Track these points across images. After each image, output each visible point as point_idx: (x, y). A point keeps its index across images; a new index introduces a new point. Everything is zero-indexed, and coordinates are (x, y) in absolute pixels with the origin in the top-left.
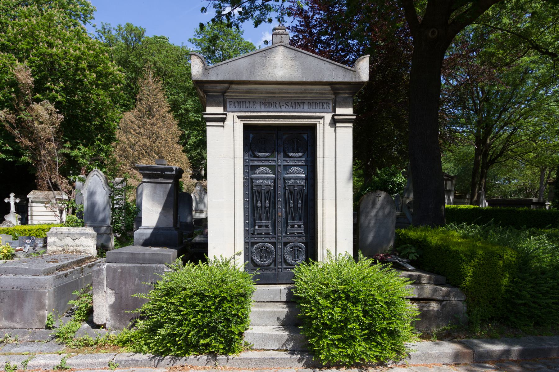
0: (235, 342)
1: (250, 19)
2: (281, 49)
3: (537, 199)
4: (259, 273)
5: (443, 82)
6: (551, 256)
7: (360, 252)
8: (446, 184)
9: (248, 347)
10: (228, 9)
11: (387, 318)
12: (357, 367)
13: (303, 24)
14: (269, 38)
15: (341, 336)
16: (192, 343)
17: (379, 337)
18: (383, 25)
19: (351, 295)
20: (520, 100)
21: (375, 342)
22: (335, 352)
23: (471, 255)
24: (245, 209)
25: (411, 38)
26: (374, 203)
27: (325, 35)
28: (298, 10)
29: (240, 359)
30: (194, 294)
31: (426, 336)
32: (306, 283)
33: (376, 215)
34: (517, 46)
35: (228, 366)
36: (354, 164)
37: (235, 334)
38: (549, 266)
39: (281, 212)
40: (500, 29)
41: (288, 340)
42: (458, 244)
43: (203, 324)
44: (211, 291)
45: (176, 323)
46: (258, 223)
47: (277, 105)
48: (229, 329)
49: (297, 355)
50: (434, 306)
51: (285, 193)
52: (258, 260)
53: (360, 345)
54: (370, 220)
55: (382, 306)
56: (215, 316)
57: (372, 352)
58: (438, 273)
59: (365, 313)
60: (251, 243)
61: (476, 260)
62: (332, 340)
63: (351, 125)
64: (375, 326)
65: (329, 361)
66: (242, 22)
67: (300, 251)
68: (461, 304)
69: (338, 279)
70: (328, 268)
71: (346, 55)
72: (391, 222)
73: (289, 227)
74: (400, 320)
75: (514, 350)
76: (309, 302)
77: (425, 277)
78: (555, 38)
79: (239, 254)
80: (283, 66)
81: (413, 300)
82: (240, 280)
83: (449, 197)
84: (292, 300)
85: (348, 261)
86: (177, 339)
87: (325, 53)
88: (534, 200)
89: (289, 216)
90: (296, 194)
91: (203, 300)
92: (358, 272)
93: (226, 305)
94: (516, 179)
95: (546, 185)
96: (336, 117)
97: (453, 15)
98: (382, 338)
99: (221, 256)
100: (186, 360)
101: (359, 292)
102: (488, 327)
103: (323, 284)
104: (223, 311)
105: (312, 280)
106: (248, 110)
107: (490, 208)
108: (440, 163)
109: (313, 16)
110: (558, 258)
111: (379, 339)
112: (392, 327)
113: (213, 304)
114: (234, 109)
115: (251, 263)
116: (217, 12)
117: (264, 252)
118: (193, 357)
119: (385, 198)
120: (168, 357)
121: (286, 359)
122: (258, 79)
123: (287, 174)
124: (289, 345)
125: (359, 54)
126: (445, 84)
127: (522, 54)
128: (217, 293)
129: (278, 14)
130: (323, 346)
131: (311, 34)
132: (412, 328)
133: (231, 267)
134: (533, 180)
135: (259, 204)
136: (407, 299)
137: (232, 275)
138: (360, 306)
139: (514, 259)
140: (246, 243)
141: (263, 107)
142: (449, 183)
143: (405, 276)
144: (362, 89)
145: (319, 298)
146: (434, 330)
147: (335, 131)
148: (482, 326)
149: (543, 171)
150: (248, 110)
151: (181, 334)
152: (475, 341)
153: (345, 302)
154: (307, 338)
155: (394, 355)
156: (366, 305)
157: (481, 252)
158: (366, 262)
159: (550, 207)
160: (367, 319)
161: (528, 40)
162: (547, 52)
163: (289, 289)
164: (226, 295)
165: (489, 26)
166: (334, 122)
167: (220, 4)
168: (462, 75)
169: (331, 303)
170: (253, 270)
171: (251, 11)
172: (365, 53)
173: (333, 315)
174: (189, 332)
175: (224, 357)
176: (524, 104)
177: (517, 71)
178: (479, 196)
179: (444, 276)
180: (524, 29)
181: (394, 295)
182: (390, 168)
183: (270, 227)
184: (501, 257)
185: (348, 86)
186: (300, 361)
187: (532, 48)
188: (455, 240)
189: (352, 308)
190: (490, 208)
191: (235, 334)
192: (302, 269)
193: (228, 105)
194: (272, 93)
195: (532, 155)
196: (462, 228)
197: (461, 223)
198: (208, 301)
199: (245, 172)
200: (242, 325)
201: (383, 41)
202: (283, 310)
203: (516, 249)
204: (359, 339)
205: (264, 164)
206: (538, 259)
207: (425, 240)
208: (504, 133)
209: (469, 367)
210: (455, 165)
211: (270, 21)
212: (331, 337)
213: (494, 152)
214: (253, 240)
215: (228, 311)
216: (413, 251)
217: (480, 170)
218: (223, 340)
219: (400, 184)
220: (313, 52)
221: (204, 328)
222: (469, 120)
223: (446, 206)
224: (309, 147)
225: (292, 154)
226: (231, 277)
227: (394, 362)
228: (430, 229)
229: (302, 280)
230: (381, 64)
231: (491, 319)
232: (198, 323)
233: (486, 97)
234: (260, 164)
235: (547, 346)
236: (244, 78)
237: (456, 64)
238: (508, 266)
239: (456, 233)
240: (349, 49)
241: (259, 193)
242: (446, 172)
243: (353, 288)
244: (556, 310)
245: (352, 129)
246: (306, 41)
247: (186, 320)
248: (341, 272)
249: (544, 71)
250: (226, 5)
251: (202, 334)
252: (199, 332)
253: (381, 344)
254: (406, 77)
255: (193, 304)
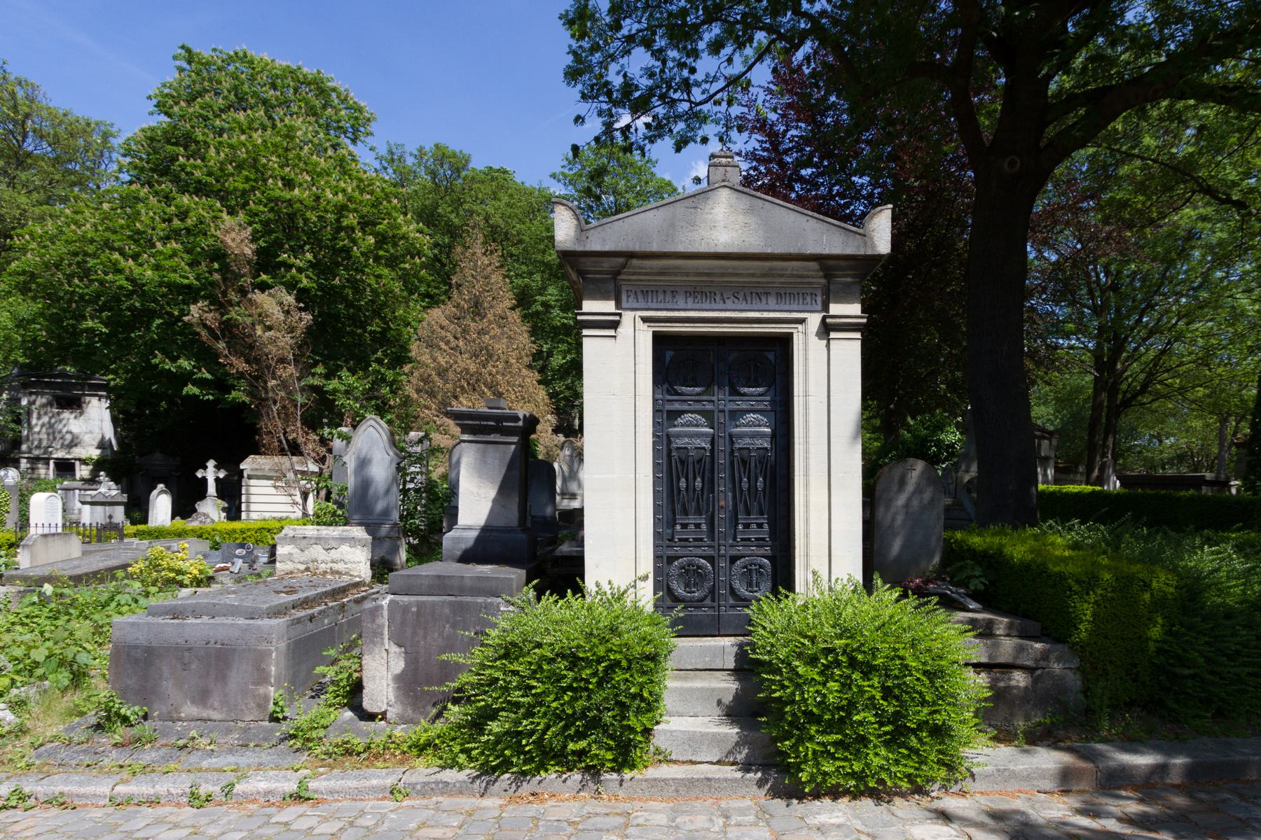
0: (635, 747)
1: (667, 138)
2: (724, 194)
3: (1213, 475)
4: (681, 615)
5: (1031, 256)
6: (1244, 584)
7: (876, 576)
8: (1039, 445)
9: (661, 757)
10: (625, 119)
11: (928, 702)
12: (871, 796)
13: (767, 145)
14: (702, 172)
15: (839, 737)
16: (552, 749)
17: (913, 738)
18: (917, 148)
19: (860, 657)
20: (1178, 288)
21: (907, 748)
22: (828, 767)
23: (1090, 582)
24: (656, 493)
25: (970, 173)
26: (902, 483)
27: (805, 167)
28: (758, 121)
29: (646, 780)
30: (557, 655)
31: (1003, 736)
32: (772, 634)
33: (907, 505)
34: (1171, 189)
35: (621, 794)
36: (865, 406)
37: (636, 733)
38: (1240, 603)
39: (724, 498)
40: (1138, 157)
41: (737, 744)
42: (1064, 560)
43: (574, 713)
44: (590, 650)
45: (522, 710)
46: (680, 519)
47: (718, 298)
48: (625, 723)
49: (756, 772)
50: (1019, 679)
51: (732, 463)
52: (680, 591)
53: (876, 754)
54: (896, 513)
55: (918, 679)
56: (598, 698)
57: (901, 768)
58: (1025, 616)
59: (887, 693)
60: (668, 557)
61: (1099, 592)
62: (823, 744)
63: (858, 335)
64: (905, 717)
65: (818, 785)
66: (652, 142)
67: (761, 574)
68: (1070, 674)
69: (833, 627)
70: (815, 607)
71: (847, 205)
72: (935, 519)
73: (740, 527)
74: (954, 705)
75: (1175, 765)
76: (778, 671)
77: (1002, 623)
78: (1243, 173)
79: (645, 578)
80: (728, 224)
81: (978, 667)
82: (647, 629)
83: (1045, 471)
84: (746, 668)
85: (854, 591)
86: (524, 742)
87: (809, 200)
88: (1209, 476)
89: (741, 507)
90: (753, 465)
91: (575, 666)
92: (872, 613)
93: (619, 676)
94: (1174, 437)
95: (1230, 447)
96: (828, 320)
97: (1051, 131)
98: (920, 740)
99: (610, 583)
100: (540, 782)
101: (874, 651)
102: (1124, 719)
103: (805, 637)
104: (614, 687)
105: (786, 629)
106: (662, 306)
107: (1123, 491)
108: (1028, 407)
109: (786, 131)
110: (1256, 588)
111: (914, 742)
112: (939, 719)
113: (595, 674)
114: (635, 306)
115: (667, 596)
116: (604, 124)
117: (692, 575)
118: (554, 776)
119: (923, 473)
120: (507, 776)
121: (735, 780)
122: (681, 248)
123: (737, 426)
124: (740, 753)
125: (874, 203)
126: (1036, 258)
127: (1180, 203)
128: (602, 654)
129: (720, 129)
130: (806, 755)
131: (782, 164)
132: (977, 720)
133: (629, 604)
134: (1204, 439)
135: (683, 484)
136: (967, 665)
137: (630, 618)
138: (876, 680)
139: (1172, 590)
140: (657, 558)
141: (690, 300)
142: (1045, 443)
143: (961, 622)
144: (878, 268)
145: (797, 663)
146: (1020, 724)
147: (828, 346)
148: (1111, 717)
149: (1224, 421)
150: (662, 306)
151: (532, 733)
152: (1099, 746)
153: (848, 672)
154: (775, 740)
155: (943, 773)
156: (887, 676)
157: (1107, 576)
158: (887, 595)
159: (1238, 491)
160: (889, 704)
161: (1192, 178)
162: (1228, 200)
163: (741, 646)
164: (618, 656)
165: (1119, 151)
166: (826, 329)
167: (610, 110)
168: (1069, 241)
169: (821, 673)
170: (671, 608)
171: (669, 122)
172: (883, 202)
173: (824, 696)
174: (548, 727)
175: (615, 776)
176: (1187, 296)
177: (1171, 234)
178: (1102, 470)
179: (1037, 621)
180: (1184, 157)
181: (941, 658)
182: (933, 415)
183: (704, 527)
184: (1146, 586)
185: (852, 263)
186: (760, 783)
187: (1199, 192)
188: (1057, 553)
189: (860, 682)
190: (1123, 491)
191: (636, 733)
192: (765, 608)
193: (624, 297)
194: (708, 275)
195: (1201, 391)
196: (1070, 529)
197: (1069, 520)
198: (584, 668)
199: (655, 424)
200: (650, 715)
201: (917, 179)
202: (728, 686)
203: (1174, 570)
204: (875, 741)
205: (692, 408)
206: (1219, 590)
207: (1000, 552)
208: (1147, 350)
209: (1087, 797)
210: (1056, 411)
211: (705, 140)
212: (820, 738)
213: (1129, 385)
214: (670, 552)
215: (623, 687)
216: (977, 573)
217: (1104, 420)
218: (612, 743)
219: (952, 446)
220: (786, 198)
221: (577, 720)
222: (1081, 329)
223: (1041, 487)
224: (778, 377)
225: (746, 390)
226: (629, 622)
227: (944, 786)
228: (1009, 531)
229: (764, 628)
230: (914, 221)
231: (1130, 704)
232: (564, 711)
233: (1113, 282)
234: (685, 407)
235: (1238, 758)
236: (655, 248)
237: (1056, 222)
238: (1160, 603)
239: (1059, 540)
240: (853, 193)
241: (682, 462)
242: (1039, 422)
243: (862, 645)
244: (1255, 687)
245: (859, 343)
246: (773, 179)
247: (541, 704)
248: (840, 614)
249: (1225, 235)
250: (621, 111)
251: (572, 731)
252: (566, 727)
253: (917, 752)
254: (961, 245)
255: (555, 674)
